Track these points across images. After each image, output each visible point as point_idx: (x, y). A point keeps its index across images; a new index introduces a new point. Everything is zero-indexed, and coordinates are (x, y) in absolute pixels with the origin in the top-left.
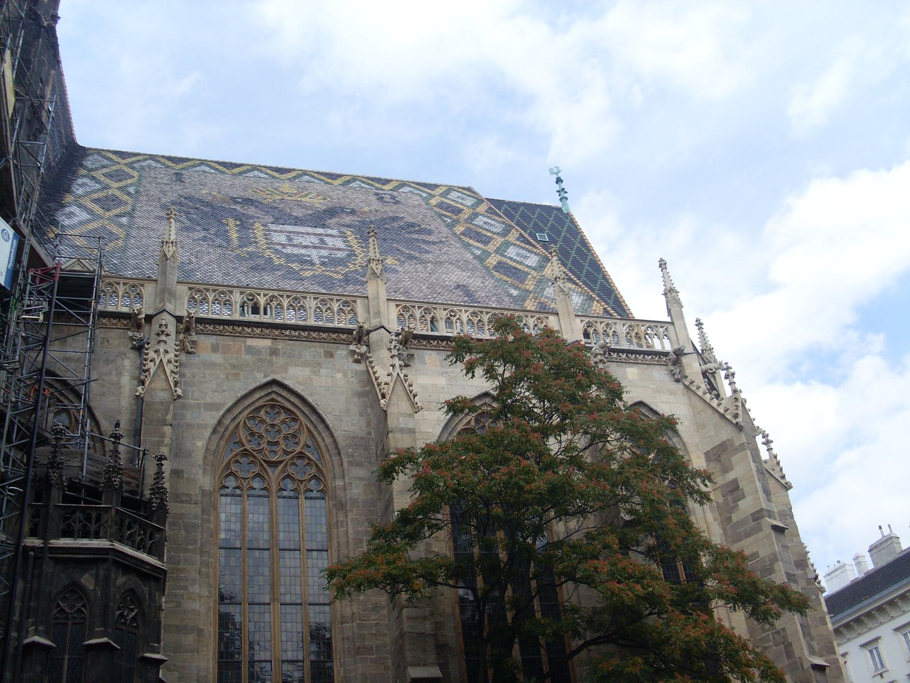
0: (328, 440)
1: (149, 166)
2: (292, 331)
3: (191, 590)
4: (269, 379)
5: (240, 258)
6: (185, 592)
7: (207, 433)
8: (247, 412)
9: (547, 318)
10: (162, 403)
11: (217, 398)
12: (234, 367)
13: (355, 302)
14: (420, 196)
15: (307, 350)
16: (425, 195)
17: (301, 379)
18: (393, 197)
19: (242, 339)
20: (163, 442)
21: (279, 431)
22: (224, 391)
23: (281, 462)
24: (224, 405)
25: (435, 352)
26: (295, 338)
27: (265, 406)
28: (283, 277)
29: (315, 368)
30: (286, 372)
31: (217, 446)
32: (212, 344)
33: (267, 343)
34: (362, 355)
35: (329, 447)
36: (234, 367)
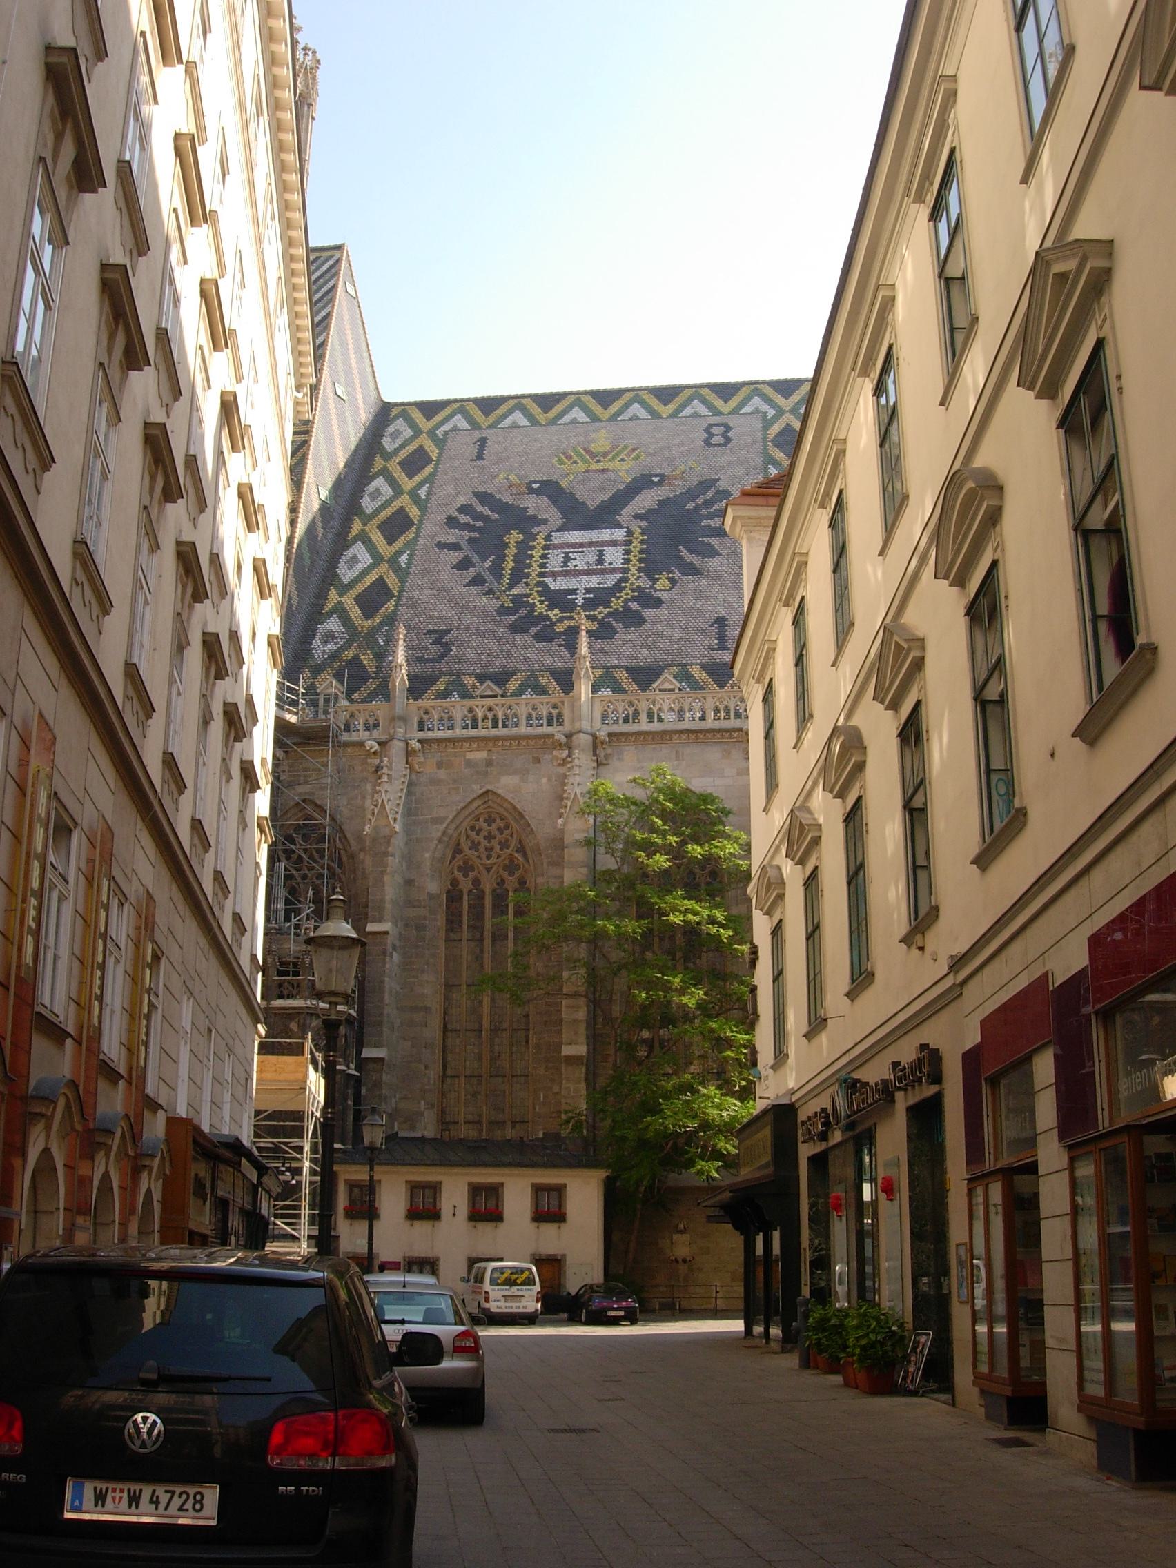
1: (455, 429)
4: (484, 790)
5: (502, 611)
14: (765, 414)
16: (771, 413)
18: (728, 428)
24: (446, 818)
28: (538, 638)
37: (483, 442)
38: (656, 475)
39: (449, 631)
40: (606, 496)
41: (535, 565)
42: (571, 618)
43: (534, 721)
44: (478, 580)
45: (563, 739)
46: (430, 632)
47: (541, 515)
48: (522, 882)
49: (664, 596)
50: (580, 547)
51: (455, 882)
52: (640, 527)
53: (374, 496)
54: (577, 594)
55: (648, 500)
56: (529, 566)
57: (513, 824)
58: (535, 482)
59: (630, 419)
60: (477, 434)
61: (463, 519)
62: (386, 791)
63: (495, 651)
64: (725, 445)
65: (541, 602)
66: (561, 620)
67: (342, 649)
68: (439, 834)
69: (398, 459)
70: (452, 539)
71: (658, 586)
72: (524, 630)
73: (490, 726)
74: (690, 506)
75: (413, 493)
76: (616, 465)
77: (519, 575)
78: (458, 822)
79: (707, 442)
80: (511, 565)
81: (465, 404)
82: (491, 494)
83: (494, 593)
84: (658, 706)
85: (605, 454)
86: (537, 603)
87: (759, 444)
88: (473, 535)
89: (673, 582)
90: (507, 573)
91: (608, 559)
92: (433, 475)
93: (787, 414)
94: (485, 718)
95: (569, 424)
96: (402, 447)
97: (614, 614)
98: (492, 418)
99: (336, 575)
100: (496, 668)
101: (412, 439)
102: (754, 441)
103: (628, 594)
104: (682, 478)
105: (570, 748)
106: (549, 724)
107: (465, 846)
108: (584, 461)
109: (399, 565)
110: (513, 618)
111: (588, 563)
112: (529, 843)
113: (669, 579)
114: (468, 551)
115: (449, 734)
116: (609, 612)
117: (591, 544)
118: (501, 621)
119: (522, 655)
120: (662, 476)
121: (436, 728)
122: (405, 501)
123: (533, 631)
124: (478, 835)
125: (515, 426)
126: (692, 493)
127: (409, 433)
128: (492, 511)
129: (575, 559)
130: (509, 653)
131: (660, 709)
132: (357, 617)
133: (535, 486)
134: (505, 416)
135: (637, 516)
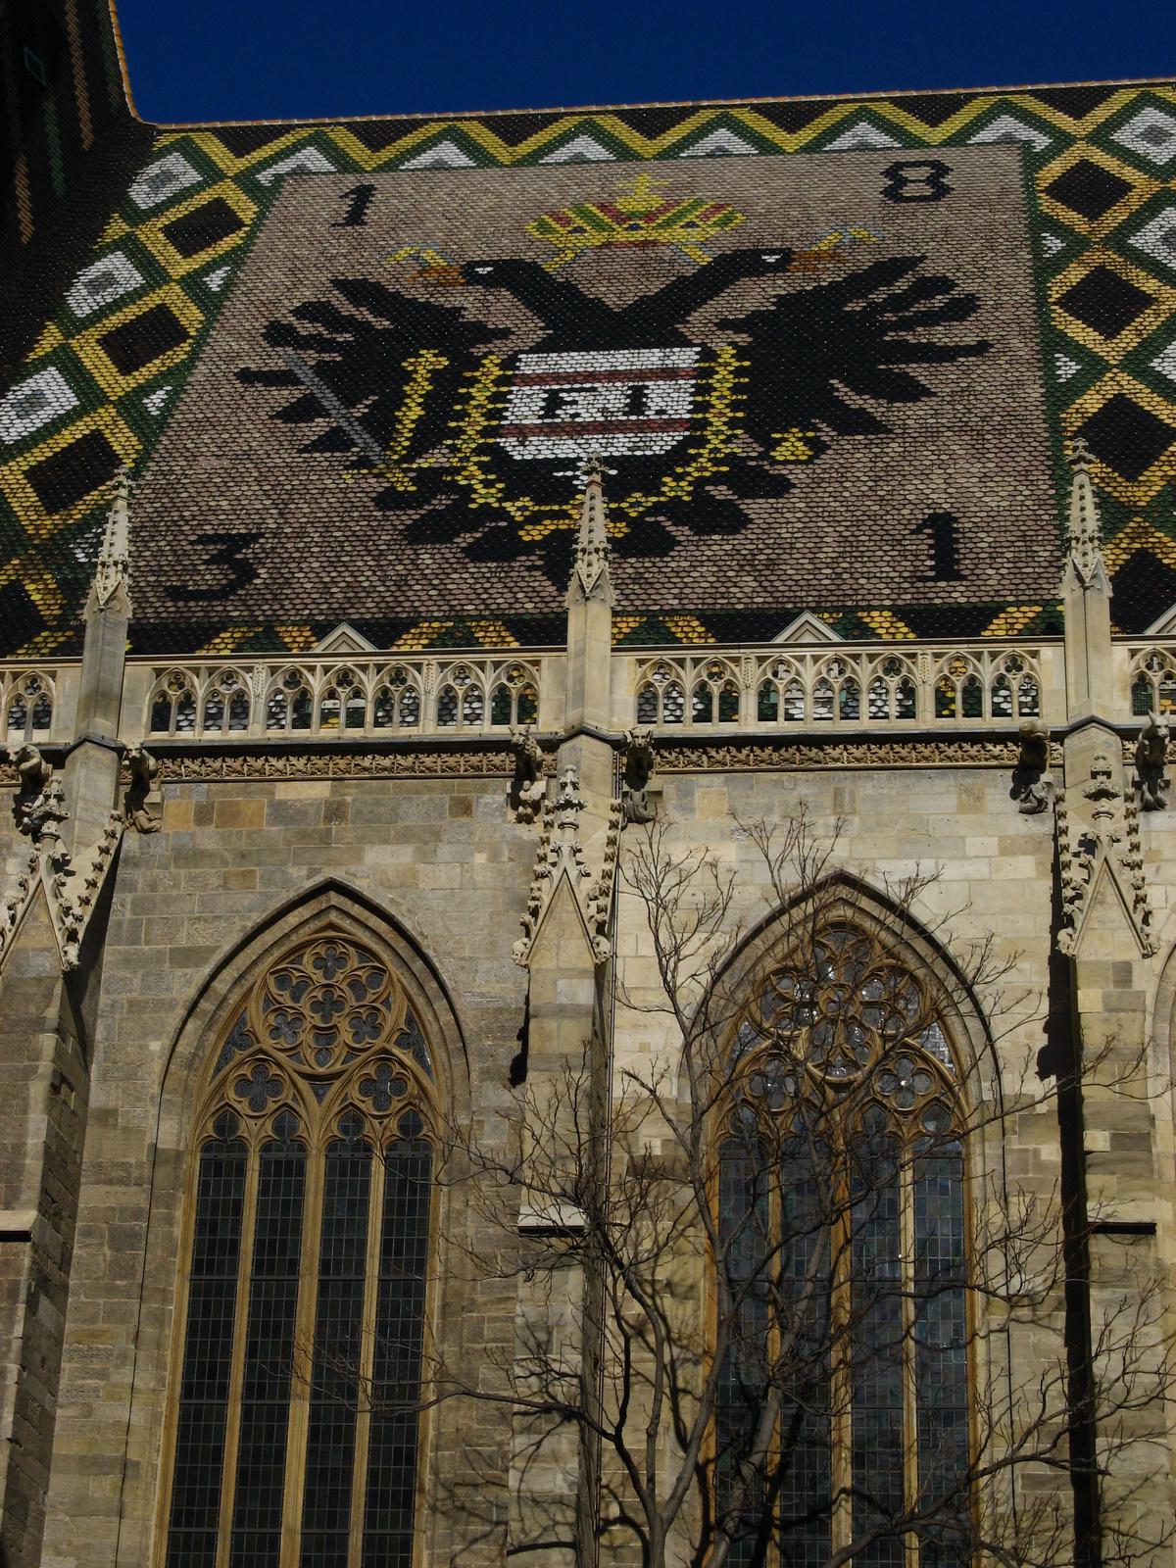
0: (446, 1017)
1: (301, 172)
2: (377, 757)
3: (115, 1378)
4: (318, 879)
5: (389, 500)
6: (102, 1383)
7: (173, 1020)
8: (270, 959)
9: (1035, 654)
10: (39, 980)
11: (202, 936)
14: (1027, 145)
15: (411, 799)
16: (1042, 142)
17: (391, 874)
18: (940, 169)
20: (35, 1069)
21: (339, 1005)
23: (336, 1076)
24: (211, 950)
25: (722, 777)
26: (386, 774)
28: (475, 553)
29: (426, 843)
31: (200, 1045)
32: (197, 805)
33: (321, 790)
35: (446, 1033)
36: (243, 856)
37: (363, 195)
38: (772, 252)
39: (255, 538)
40: (655, 287)
41: (476, 414)
44: (334, 441)
46: (205, 540)
47: (495, 322)
48: (411, 1125)
49: (797, 475)
51: (226, 1122)
52: (733, 344)
55: (754, 296)
58: (484, 264)
59: (708, 156)
60: (351, 181)
61: (305, 328)
64: (935, 197)
65: (487, 484)
66: (535, 519)
69: (160, 224)
71: (779, 454)
72: (447, 537)
74: (855, 306)
75: (193, 284)
76: (678, 233)
77: (432, 431)
79: (893, 193)
80: (416, 412)
83: (371, 466)
85: (649, 216)
86: (478, 487)
87: (1018, 196)
88: (326, 357)
89: (817, 447)
93: (1081, 144)
95: (566, 163)
97: (674, 509)
98: (386, 154)
100: (369, 609)
102: (1004, 191)
103: (706, 469)
104: (834, 255)
107: (258, 1020)
108: (600, 226)
112: (436, 1020)
113: (807, 441)
114: (311, 384)
117: (613, 376)
118: (386, 518)
119: (434, 587)
120: (787, 256)
122: (172, 296)
123: (465, 539)
126: (859, 283)
127: (193, 176)
129: (575, 402)
130: (402, 583)
132: (26, 509)
135: (724, 325)
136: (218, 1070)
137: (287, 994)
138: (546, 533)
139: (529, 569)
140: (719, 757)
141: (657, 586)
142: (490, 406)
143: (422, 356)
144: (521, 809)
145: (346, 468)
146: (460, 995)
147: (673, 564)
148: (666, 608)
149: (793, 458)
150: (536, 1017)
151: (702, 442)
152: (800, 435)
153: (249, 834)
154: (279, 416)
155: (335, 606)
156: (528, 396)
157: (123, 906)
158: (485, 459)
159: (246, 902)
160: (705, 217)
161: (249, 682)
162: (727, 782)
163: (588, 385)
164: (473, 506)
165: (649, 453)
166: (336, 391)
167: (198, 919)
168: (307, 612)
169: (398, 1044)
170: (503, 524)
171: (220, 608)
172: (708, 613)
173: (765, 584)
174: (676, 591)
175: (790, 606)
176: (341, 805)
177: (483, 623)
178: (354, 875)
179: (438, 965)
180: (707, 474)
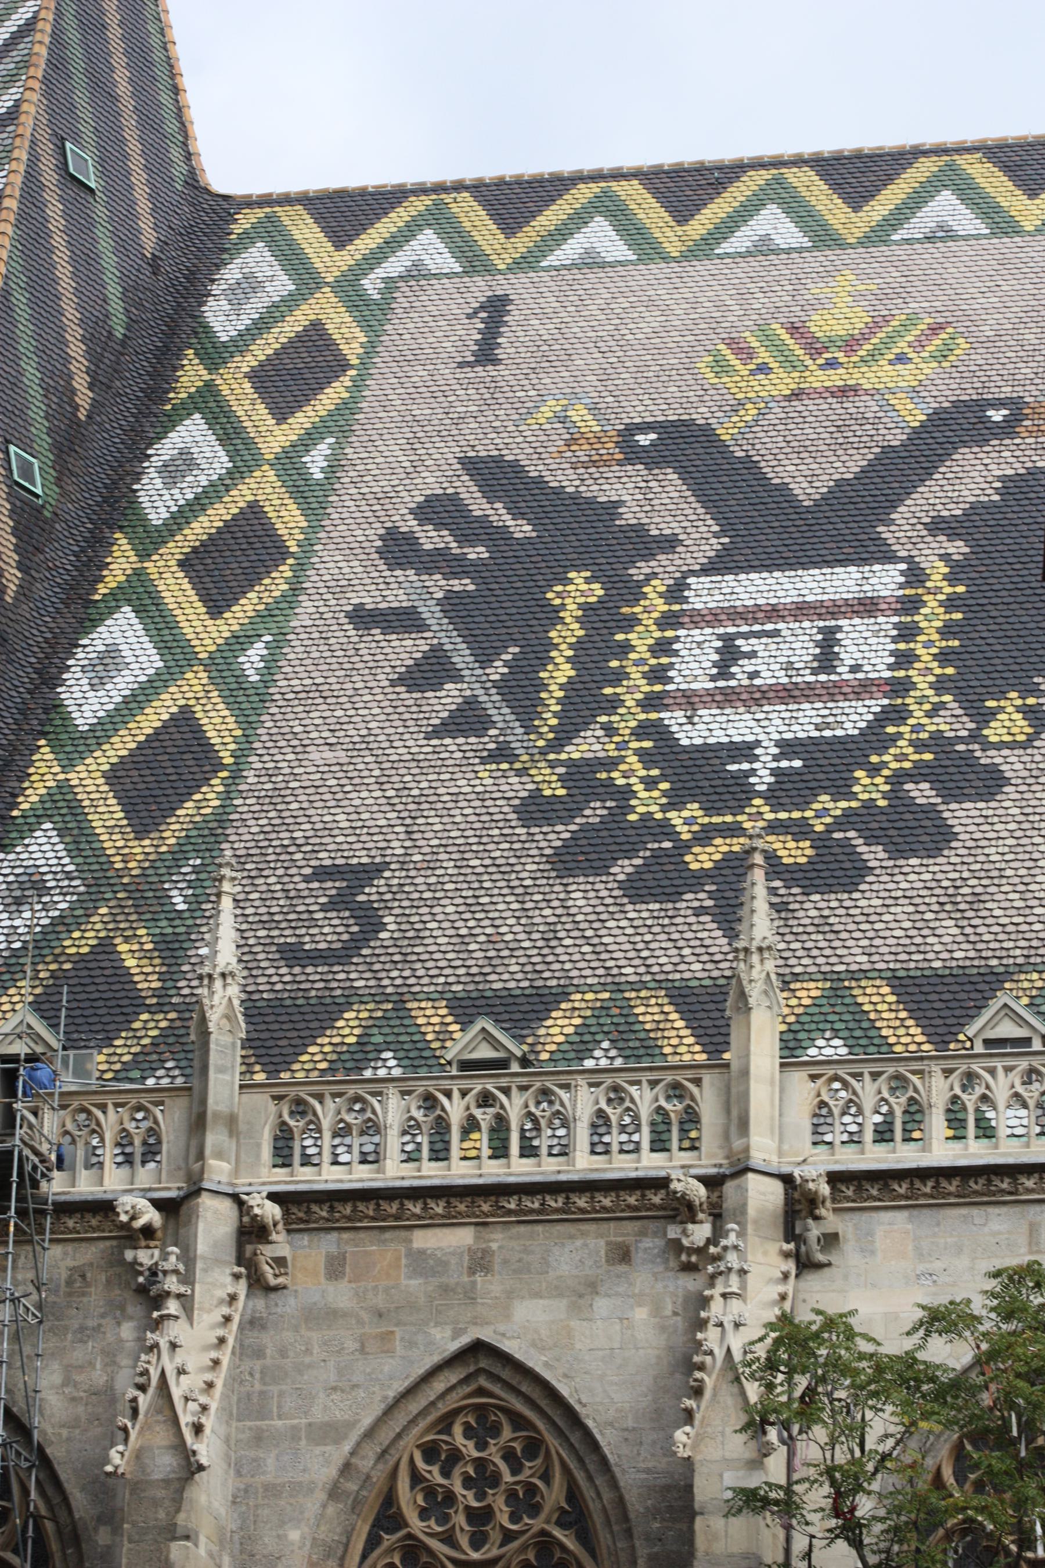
0: (607, 1495)
1: (417, 274)
4: (465, 1340)
8: (416, 1431)
12: (380, 1315)
13: (697, 1082)
15: (563, 1244)
17: (544, 1333)
19: (403, 1234)
21: (495, 1480)
22: (355, 1386)
25: (904, 1215)
27: (455, 1413)
29: (581, 1296)
30: (507, 1315)
32: (327, 1256)
34: (700, 1251)
39: (378, 870)
40: (852, 465)
42: (735, 830)
43: (615, 1139)
45: (699, 1192)
46: (322, 874)
47: (660, 526)
49: (1011, 763)
50: (769, 619)
52: (945, 557)
53: (172, 473)
54: (756, 758)
56: (619, 677)
57: (552, 1442)
58: (645, 427)
60: (480, 289)
61: (431, 538)
62: (174, 1346)
63: (510, 929)
65: (650, 783)
66: (704, 836)
67: (63, 924)
68: (332, 1472)
69: (247, 362)
70: (397, 598)
71: (994, 732)
72: (601, 869)
73: (486, 1152)
78: (386, 1435)
80: (564, 672)
81: (448, 198)
82: (515, 465)
84: (979, 1090)
85: (851, 344)
86: (639, 787)
88: (457, 585)
90: (553, 697)
91: (848, 653)
92: (347, 409)
94: (471, 1125)
95: (749, 253)
96: (261, 325)
98: (523, 241)
99: (58, 706)
101: (290, 302)
105: (717, 1216)
106: (659, 1145)
107: (408, 1500)
108: (790, 363)
109: (240, 678)
110: (564, 831)
111: (789, 666)
113: (1027, 712)
115: (362, 1177)
116: (847, 813)
117: (801, 610)
121: (327, 1157)
123: (623, 869)
124: (446, 1473)
125: (591, 262)
127: (282, 285)
128: (516, 513)
129: (753, 655)
130: (551, 936)
131: (984, 1098)
133: (644, 439)
134: (561, 234)
135: (938, 526)
136: (364, 1557)
137: (435, 1469)
138: (718, 857)
139: (699, 912)
140: (902, 1191)
141: (844, 935)
142: (653, 662)
143: (571, 581)
144: (684, 1257)
145: (484, 761)
146: (624, 1471)
147: (862, 903)
148: (854, 967)
149: (1007, 738)
150: (702, 1514)
151: (899, 715)
152: (1019, 702)
153: (386, 1290)
154: (401, 681)
155: (474, 970)
156: (699, 644)
157: (251, 1374)
158: (647, 744)
159: (386, 1369)
160: (919, 344)
161: (377, 1106)
162: (910, 1220)
163: (769, 627)
164: (632, 817)
165: (839, 733)
166: (471, 639)
167: (334, 1389)
168: (442, 980)
169: (560, 1524)
170: (667, 845)
171: (342, 976)
172: (901, 974)
173: (968, 930)
174: (865, 943)
175: (994, 962)
176: (486, 1252)
177: (643, 993)
178: (503, 1335)
179: (598, 1437)
180: (907, 765)
